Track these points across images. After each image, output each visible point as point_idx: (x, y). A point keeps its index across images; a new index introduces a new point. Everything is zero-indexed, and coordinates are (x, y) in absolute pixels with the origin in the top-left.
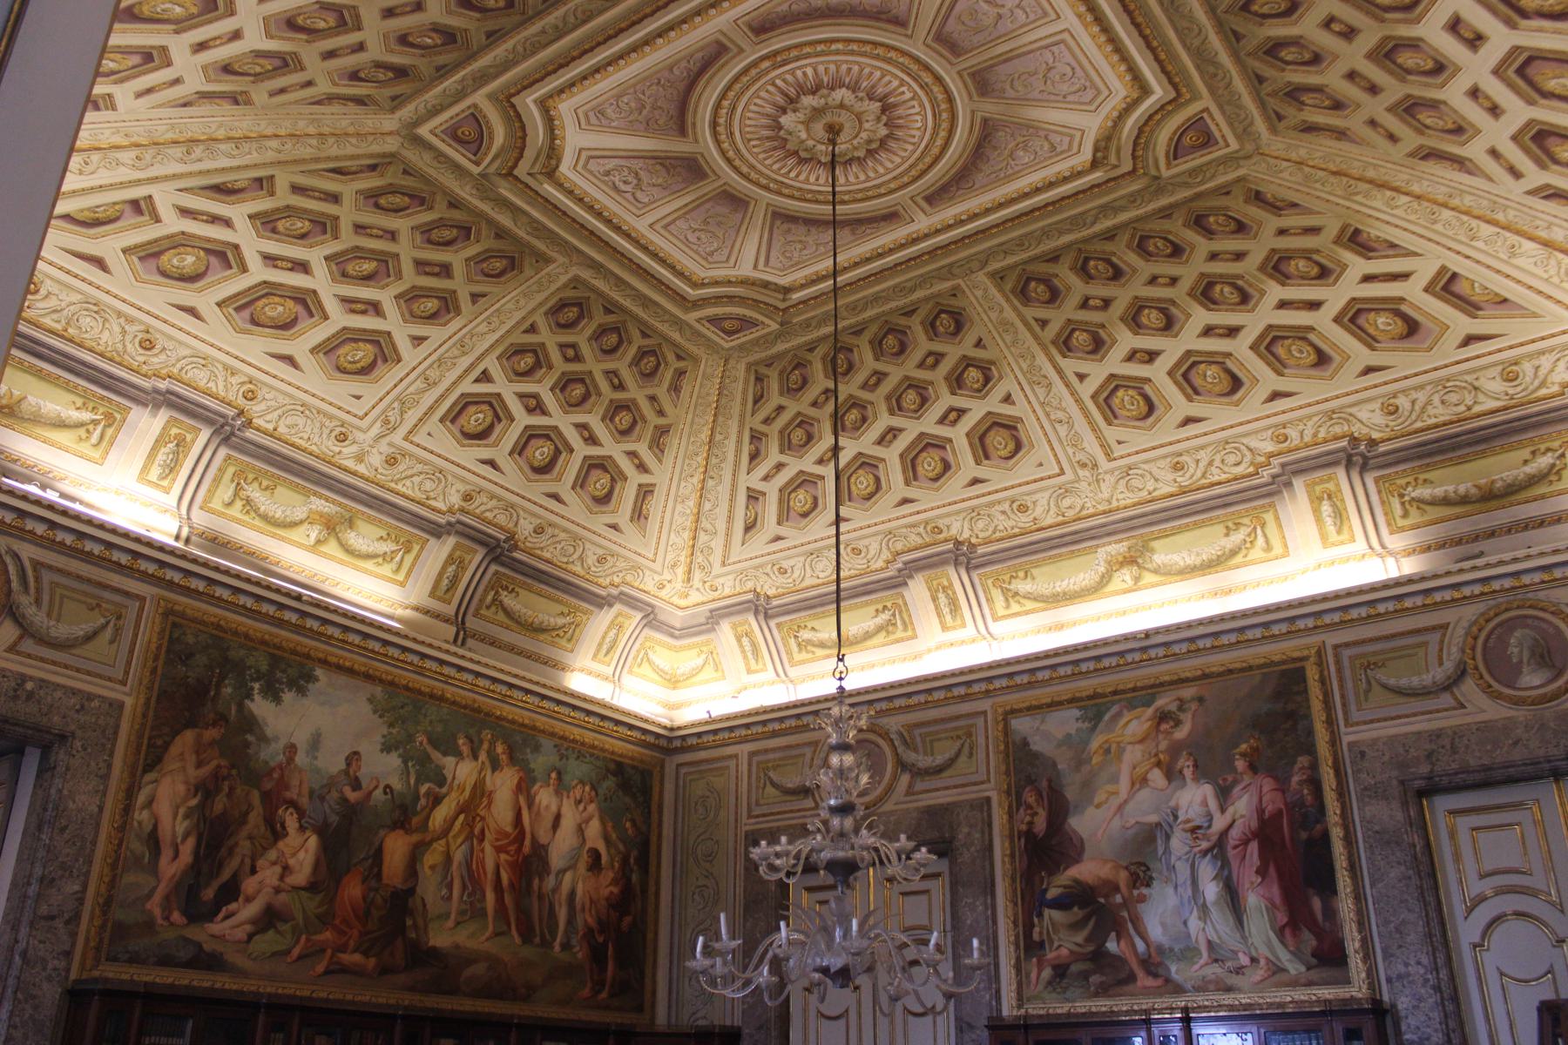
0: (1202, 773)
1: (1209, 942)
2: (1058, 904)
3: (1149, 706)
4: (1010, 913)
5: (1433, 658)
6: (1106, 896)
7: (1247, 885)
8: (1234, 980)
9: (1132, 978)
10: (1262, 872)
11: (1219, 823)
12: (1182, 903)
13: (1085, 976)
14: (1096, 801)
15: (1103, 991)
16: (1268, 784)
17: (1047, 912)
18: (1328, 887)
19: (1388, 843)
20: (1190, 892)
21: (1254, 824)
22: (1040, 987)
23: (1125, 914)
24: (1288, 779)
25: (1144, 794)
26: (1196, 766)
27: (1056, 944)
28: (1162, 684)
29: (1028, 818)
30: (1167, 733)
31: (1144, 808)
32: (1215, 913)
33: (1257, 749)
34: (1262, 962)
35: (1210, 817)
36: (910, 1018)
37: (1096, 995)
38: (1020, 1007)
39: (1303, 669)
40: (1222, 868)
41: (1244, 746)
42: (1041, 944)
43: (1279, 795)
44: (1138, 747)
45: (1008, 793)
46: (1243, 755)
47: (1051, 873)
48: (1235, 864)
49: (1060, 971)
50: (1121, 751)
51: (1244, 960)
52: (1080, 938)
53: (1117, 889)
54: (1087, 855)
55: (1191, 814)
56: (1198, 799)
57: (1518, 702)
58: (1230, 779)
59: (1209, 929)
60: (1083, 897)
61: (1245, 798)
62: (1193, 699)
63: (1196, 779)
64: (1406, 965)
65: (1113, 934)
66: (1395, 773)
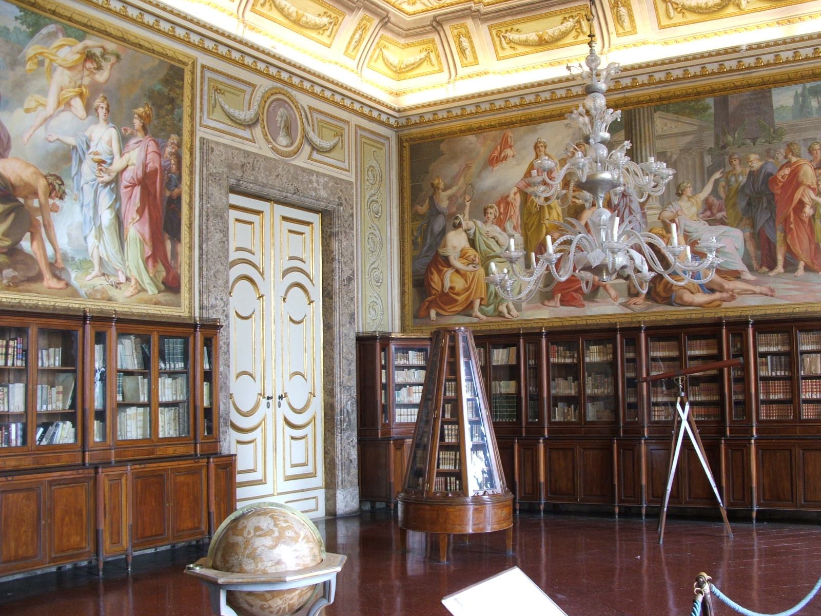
0: (112, 117)
1: (101, 258)
3: (81, 41)
5: (246, 104)
6: (26, 197)
7: (130, 220)
8: (113, 292)
9: (39, 277)
10: (140, 212)
11: (118, 164)
14: (26, 106)
16: (152, 147)
18: (176, 236)
19: (217, 216)
20: (91, 213)
21: (140, 174)
23: (40, 218)
24: (165, 147)
25: (66, 116)
26: (108, 110)
28: (92, 28)
30: (91, 73)
33: (148, 116)
34: (133, 282)
39: (182, 71)
41: (141, 110)
43: (157, 157)
44: (67, 72)
46: (140, 116)
48: (124, 200)
50: (51, 71)
51: (122, 279)
53: (35, 194)
54: (13, 152)
55: (100, 149)
56: (106, 138)
57: (274, 149)
58: (129, 132)
59: (101, 248)
61: (137, 150)
62: (113, 54)
64: (216, 299)
65: (28, 235)
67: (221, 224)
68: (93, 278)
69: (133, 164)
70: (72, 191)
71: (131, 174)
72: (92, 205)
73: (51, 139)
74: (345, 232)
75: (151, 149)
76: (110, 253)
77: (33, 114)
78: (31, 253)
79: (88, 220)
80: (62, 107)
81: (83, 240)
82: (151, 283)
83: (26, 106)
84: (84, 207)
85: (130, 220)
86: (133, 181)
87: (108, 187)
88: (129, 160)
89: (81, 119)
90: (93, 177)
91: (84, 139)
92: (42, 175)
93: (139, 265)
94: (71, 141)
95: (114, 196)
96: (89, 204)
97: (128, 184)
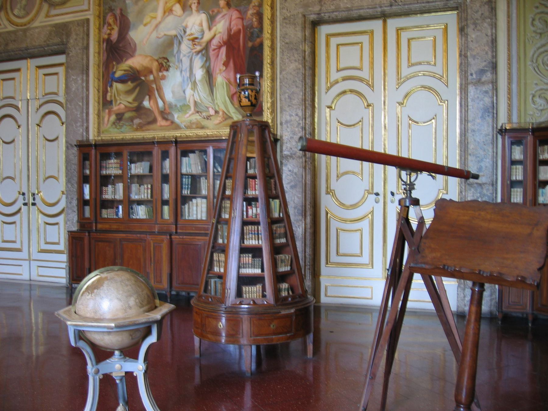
1: (195, 103)
2: (122, 80)
4: (96, 85)
6: (145, 76)
7: (218, 71)
8: (205, 123)
9: (155, 121)
10: (226, 64)
11: (207, 36)
12: (183, 80)
13: (132, 119)
14: (145, 22)
15: (140, 127)
16: (235, 14)
17: (115, 84)
19: (292, 49)
20: (188, 74)
21: (225, 37)
22: (109, 125)
23: (154, 86)
24: (246, 12)
25: (170, 19)
27: (118, 102)
29: (108, 32)
31: (169, 26)
32: (199, 86)
34: (221, 113)
35: (203, 32)
36: (47, 142)
37: (137, 130)
38: (98, 136)
40: (206, 61)
42: (111, 102)
43: (240, 21)
45: (99, 17)
47: (118, 63)
48: (213, 59)
49: (120, 117)
51: (212, 112)
52: (130, 99)
53: (151, 72)
54: (138, 52)
55: (193, 31)
56: (198, 22)
58: (216, 11)
60: (134, 77)
61: (223, 22)
63: (198, 11)
64: (291, 116)
66: (301, 10)
67: (296, 56)
68: (190, 116)
69: (220, 33)
70: (174, 64)
71: (219, 40)
72: (188, 69)
73: (160, 36)
74: (475, 24)
75: (234, 17)
76: (202, 97)
77: (149, 26)
78: (150, 108)
79: (186, 79)
80: (167, 14)
81: (182, 93)
82: (237, 112)
83: (145, 22)
84: (183, 73)
85: (218, 71)
86: (219, 44)
87: (200, 55)
88: (216, 31)
89: (179, 16)
90: (189, 50)
91: (182, 29)
92: (155, 60)
93: (225, 101)
94: (173, 33)
95: (205, 59)
96: (186, 69)
97: (215, 47)
